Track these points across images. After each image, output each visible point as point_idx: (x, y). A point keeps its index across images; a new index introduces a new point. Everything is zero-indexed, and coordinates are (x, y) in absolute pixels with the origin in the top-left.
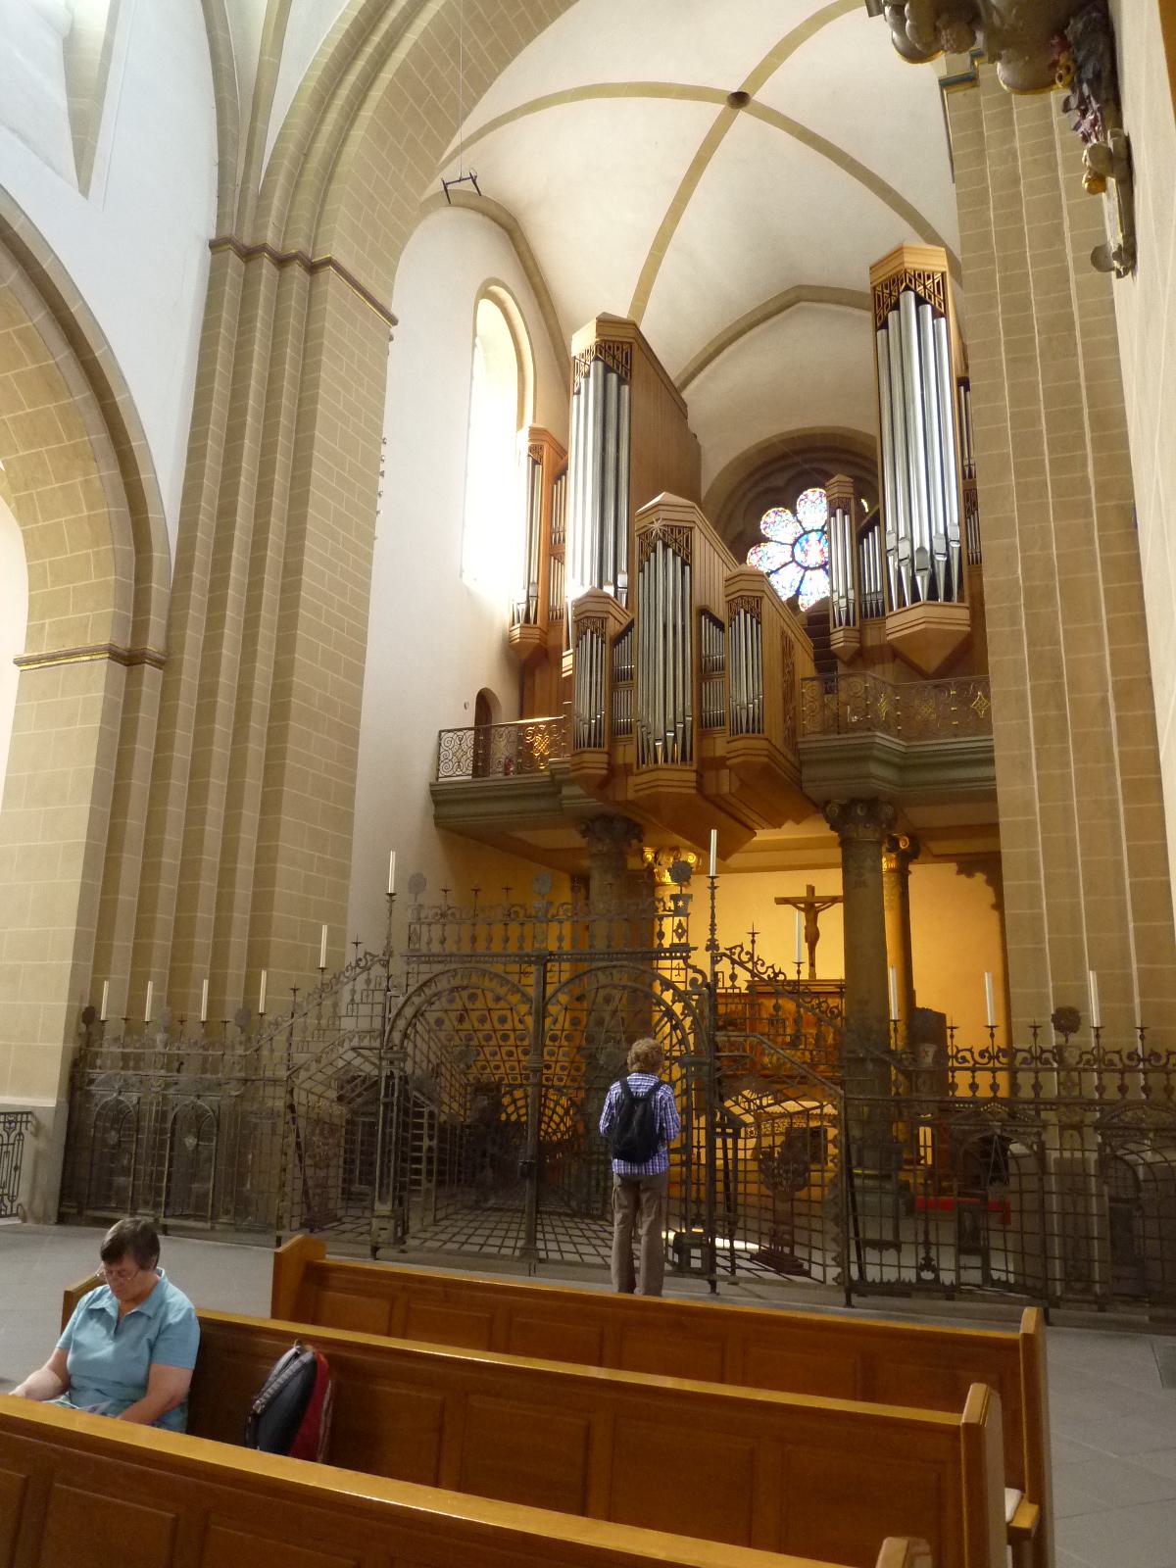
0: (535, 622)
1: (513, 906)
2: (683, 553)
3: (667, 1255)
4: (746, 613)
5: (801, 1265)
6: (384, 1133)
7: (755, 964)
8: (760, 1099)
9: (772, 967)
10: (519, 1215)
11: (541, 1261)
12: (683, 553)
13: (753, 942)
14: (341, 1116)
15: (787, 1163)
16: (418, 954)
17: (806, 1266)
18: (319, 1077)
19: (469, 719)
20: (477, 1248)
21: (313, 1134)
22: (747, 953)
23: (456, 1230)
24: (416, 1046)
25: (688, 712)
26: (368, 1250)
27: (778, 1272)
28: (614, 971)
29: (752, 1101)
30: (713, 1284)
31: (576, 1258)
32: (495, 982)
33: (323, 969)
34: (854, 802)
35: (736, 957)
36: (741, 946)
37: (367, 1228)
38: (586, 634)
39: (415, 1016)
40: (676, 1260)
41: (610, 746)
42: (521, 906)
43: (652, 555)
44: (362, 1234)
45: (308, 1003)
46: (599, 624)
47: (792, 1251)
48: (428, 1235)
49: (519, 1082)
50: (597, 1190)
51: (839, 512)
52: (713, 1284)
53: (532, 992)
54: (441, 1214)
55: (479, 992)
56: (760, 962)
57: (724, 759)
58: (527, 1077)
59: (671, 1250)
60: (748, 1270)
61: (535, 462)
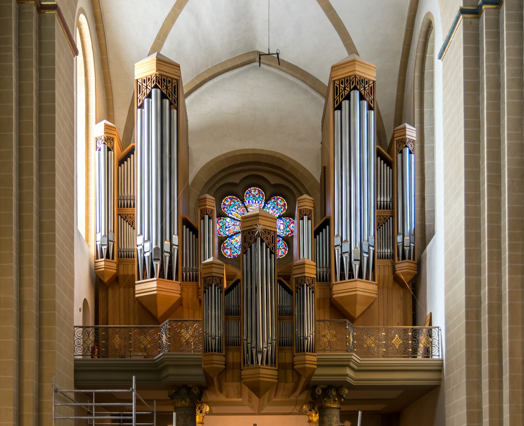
2: (271, 246)
4: (307, 286)
12: (271, 246)
38: (211, 286)
41: (226, 352)
43: (253, 245)
61: (109, 149)
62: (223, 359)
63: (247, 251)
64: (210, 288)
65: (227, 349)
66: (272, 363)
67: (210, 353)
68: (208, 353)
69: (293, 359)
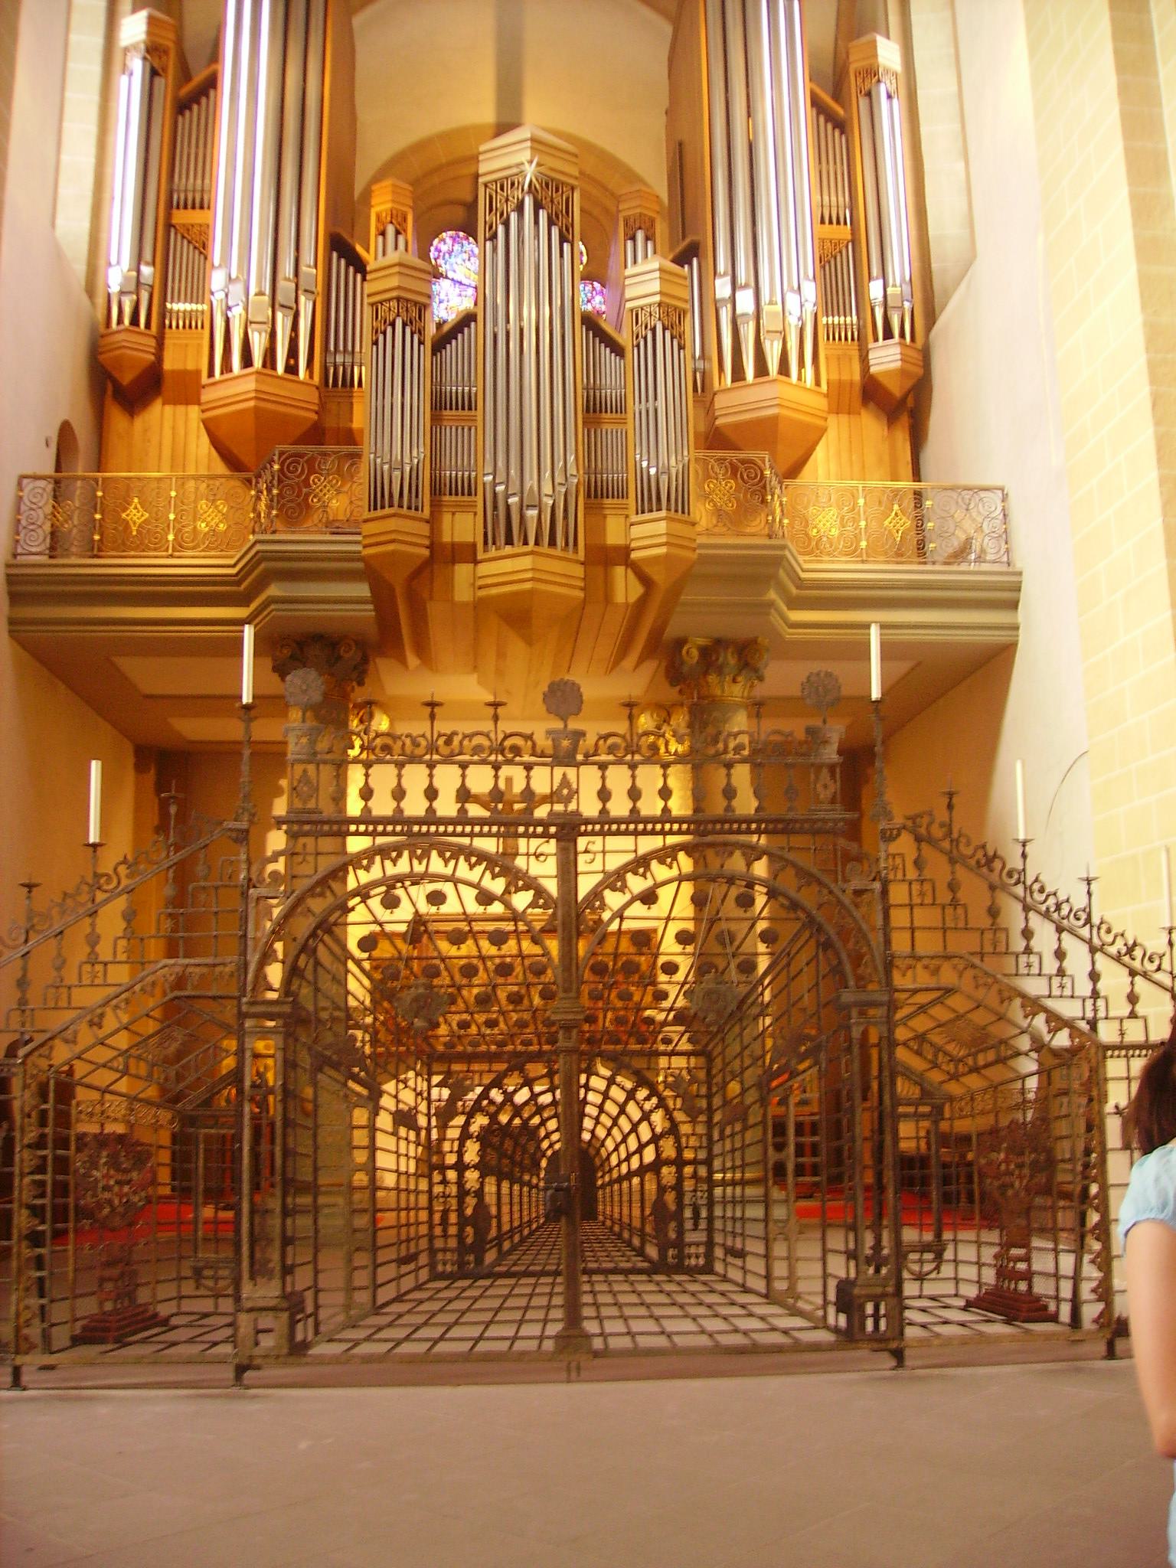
0: (148, 325)
1: (506, 737)
2: (562, 221)
3: (825, 1317)
5: (1045, 1308)
6: (255, 1155)
7: (955, 842)
8: (975, 1055)
9: (984, 847)
10: (550, 1280)
11: (596, 1354)
13: (950, 807)
14: (156, 1127)
15: (1022, 1154)
16: (314, 817)
17: (1052, 1307)
18: (102, 1055)
19: (46, 465)
20: (465, 1347)
21: (95, 1165)
22: (942, 825)
23: (421, 1319)
24: (317, 990)
25: (571, 470)
26: (229, 1373)
27: (1008, 1322)
28: (710, 853)
29: (960, 1060)
30: (899, 1355)
31: (661, 1342)
32: (480, 869)
33: (95, 846)
34: (719, 643)
35: (923, 831)
36: (930, 814)
37: (229, 1332)
38: (393, 324)
39: (313, 935)
40: (842, 1320)
41: (432, 513)
42: (529, 737)
43: (514, 217)
44: (215, 1344)
45: (63, 913)
46: (414, 314)
47: (1030, 1287)
48: (361, 1334)
49: (535, 1048)
50: (696, 1227)
51: (640, 235)
52: (899, 1355)
53: (552, 887)
54: (385, 1294)
55: (447, 888)
56: (963, 840)
57: (627, 550)
58: (552, 1041)
59: (831, 1310)
60: (962, 1324)
61: (154, 73)
62: (425, 529)
63: (496, 234)
64: (389, 330)
65: (436, 506)
66: (567, 544)
67: (387, 511)
68: (379, 513)
69: (627, 532)
